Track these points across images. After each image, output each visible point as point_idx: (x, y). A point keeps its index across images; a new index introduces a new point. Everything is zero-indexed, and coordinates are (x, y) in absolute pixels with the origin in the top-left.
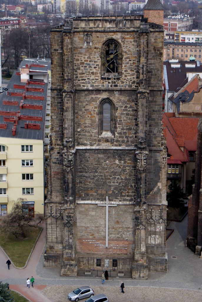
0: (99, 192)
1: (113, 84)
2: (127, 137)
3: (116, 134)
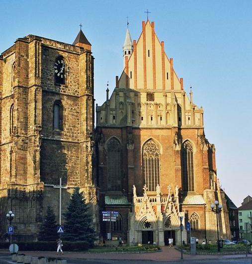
1: (63, 90)
2: (73, 133)
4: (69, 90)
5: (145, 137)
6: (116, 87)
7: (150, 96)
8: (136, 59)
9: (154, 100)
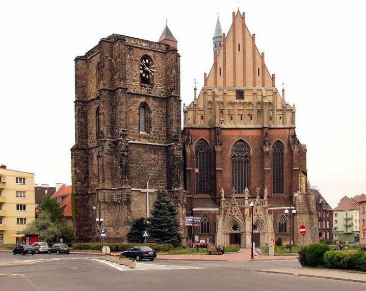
0: (140, 181)
3: (151, 133)
4: (155, 91)
5: (234, 138)
6: (205, 85)
7: (240, 94)
8: (225, 54)
9: (243, 99)
